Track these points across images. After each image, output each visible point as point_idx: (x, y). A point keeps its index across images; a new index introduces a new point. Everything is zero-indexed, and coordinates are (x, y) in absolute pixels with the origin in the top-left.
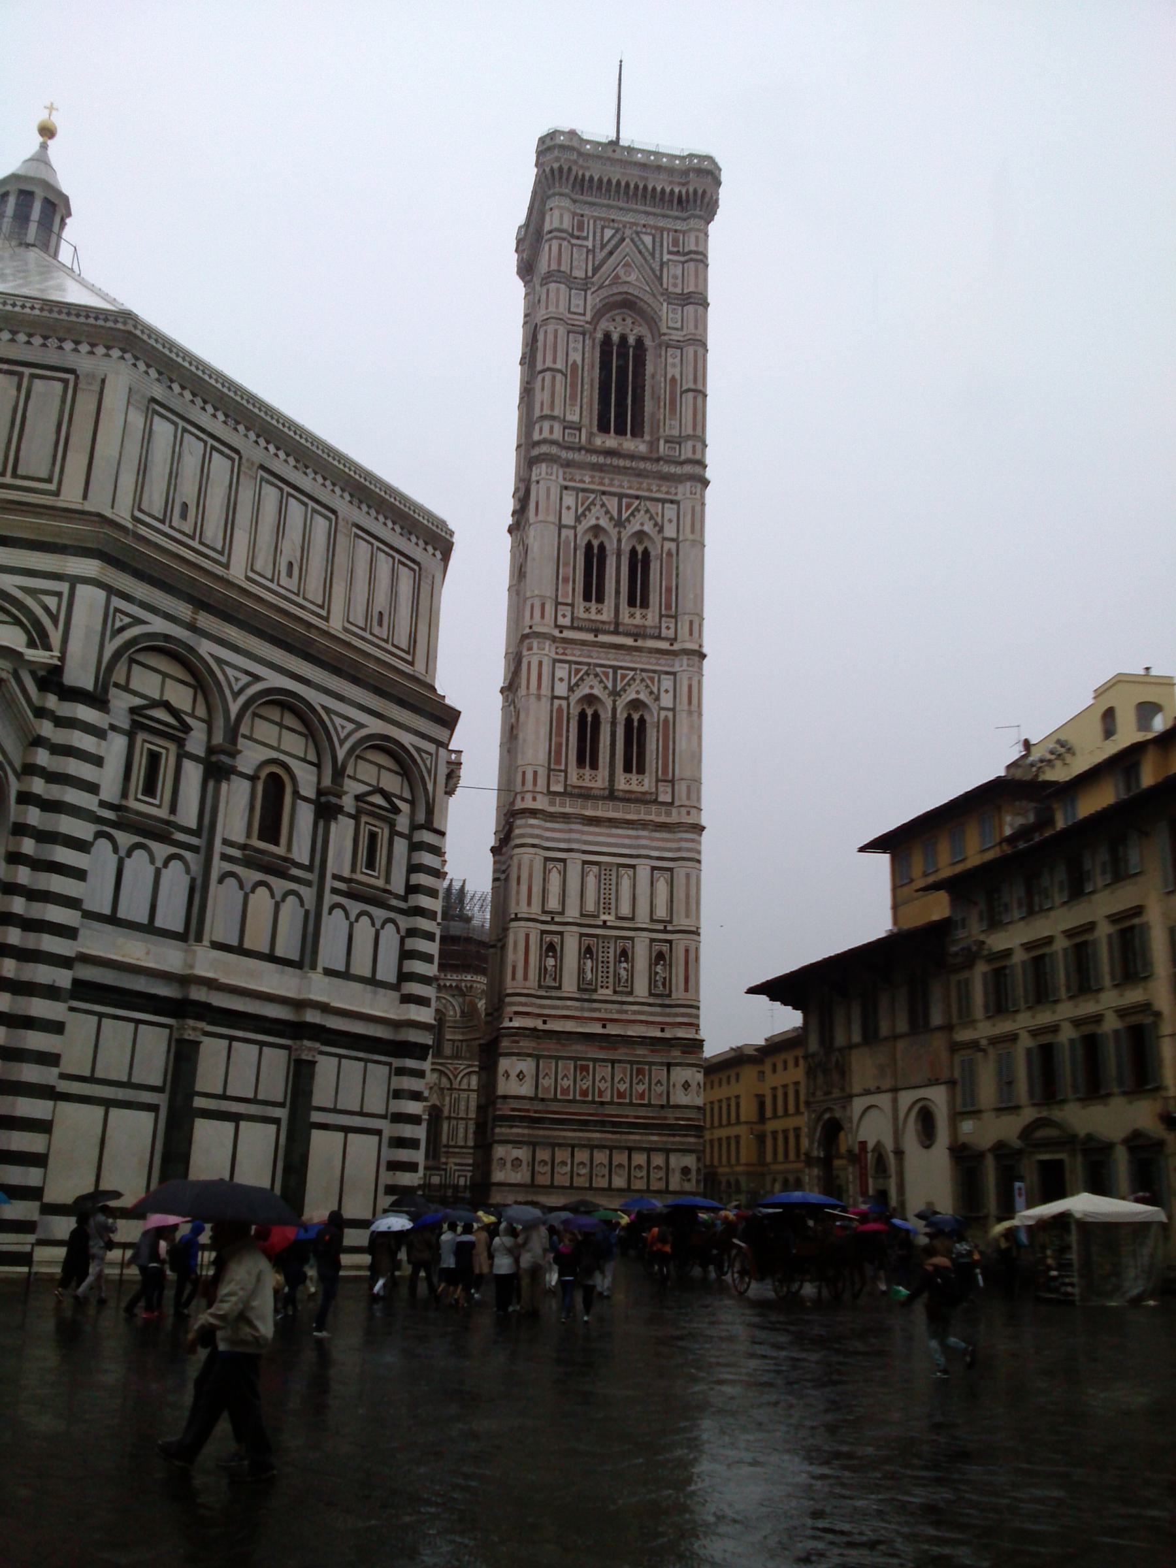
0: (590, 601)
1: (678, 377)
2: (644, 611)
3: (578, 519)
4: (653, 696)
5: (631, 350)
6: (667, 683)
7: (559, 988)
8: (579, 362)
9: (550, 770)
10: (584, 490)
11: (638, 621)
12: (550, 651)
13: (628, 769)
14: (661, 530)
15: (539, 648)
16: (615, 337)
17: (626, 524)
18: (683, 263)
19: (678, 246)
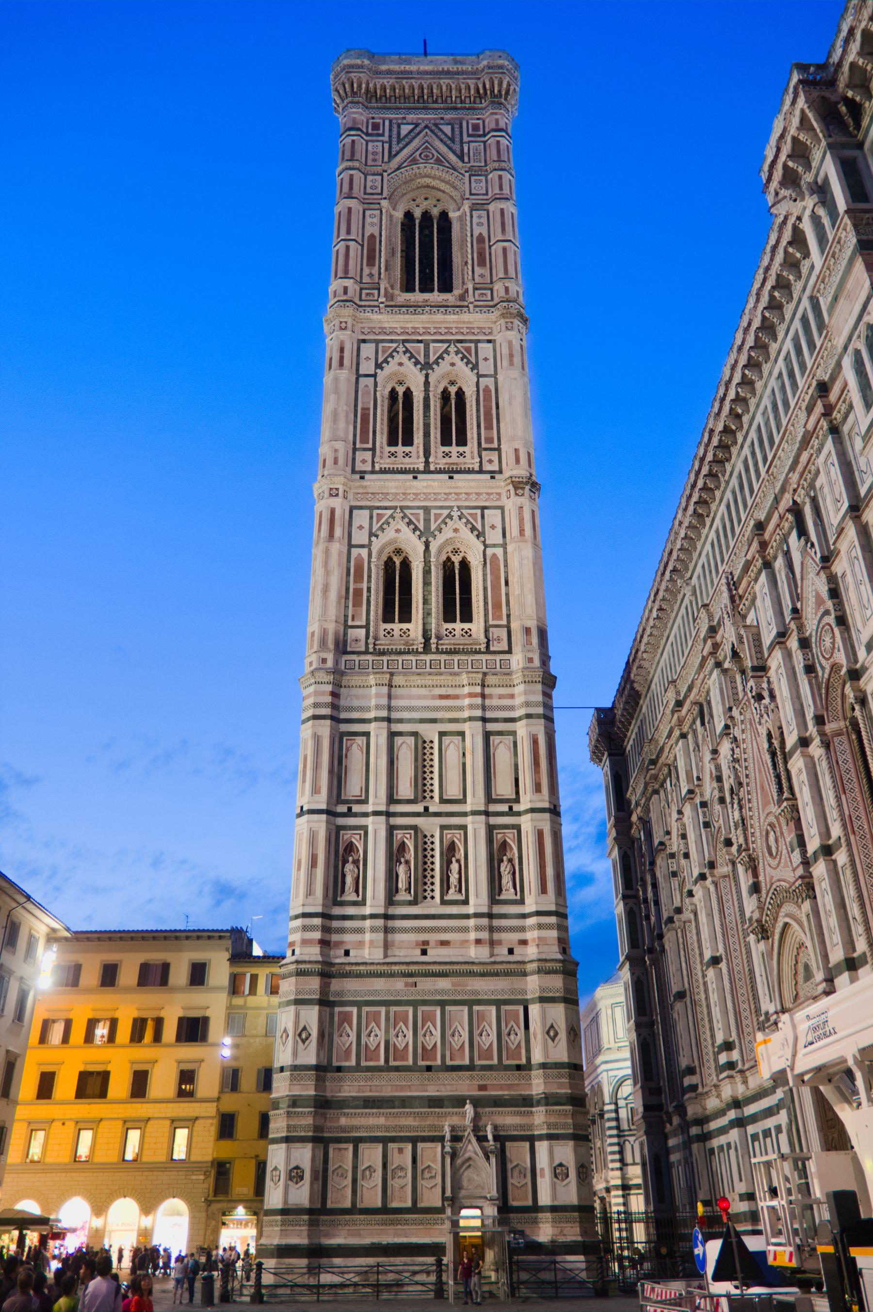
0: (396, 445)
1: (485, 235)
2: (461, 449)
3: (378, 366)
4: (476, 533)
5: (435, 222)
6: (493, 517)
7: (363, 903)
8: (377, 234)
9: (346, 626)
10: (383, 341)
11: (454, 459)
12: (345, 497)
13: (449, 616)
14: (475, 367)
15: (331, 495)
16: (417, 213)
17: (435, 366)
18: (485, 142)
19: (478, 130)
